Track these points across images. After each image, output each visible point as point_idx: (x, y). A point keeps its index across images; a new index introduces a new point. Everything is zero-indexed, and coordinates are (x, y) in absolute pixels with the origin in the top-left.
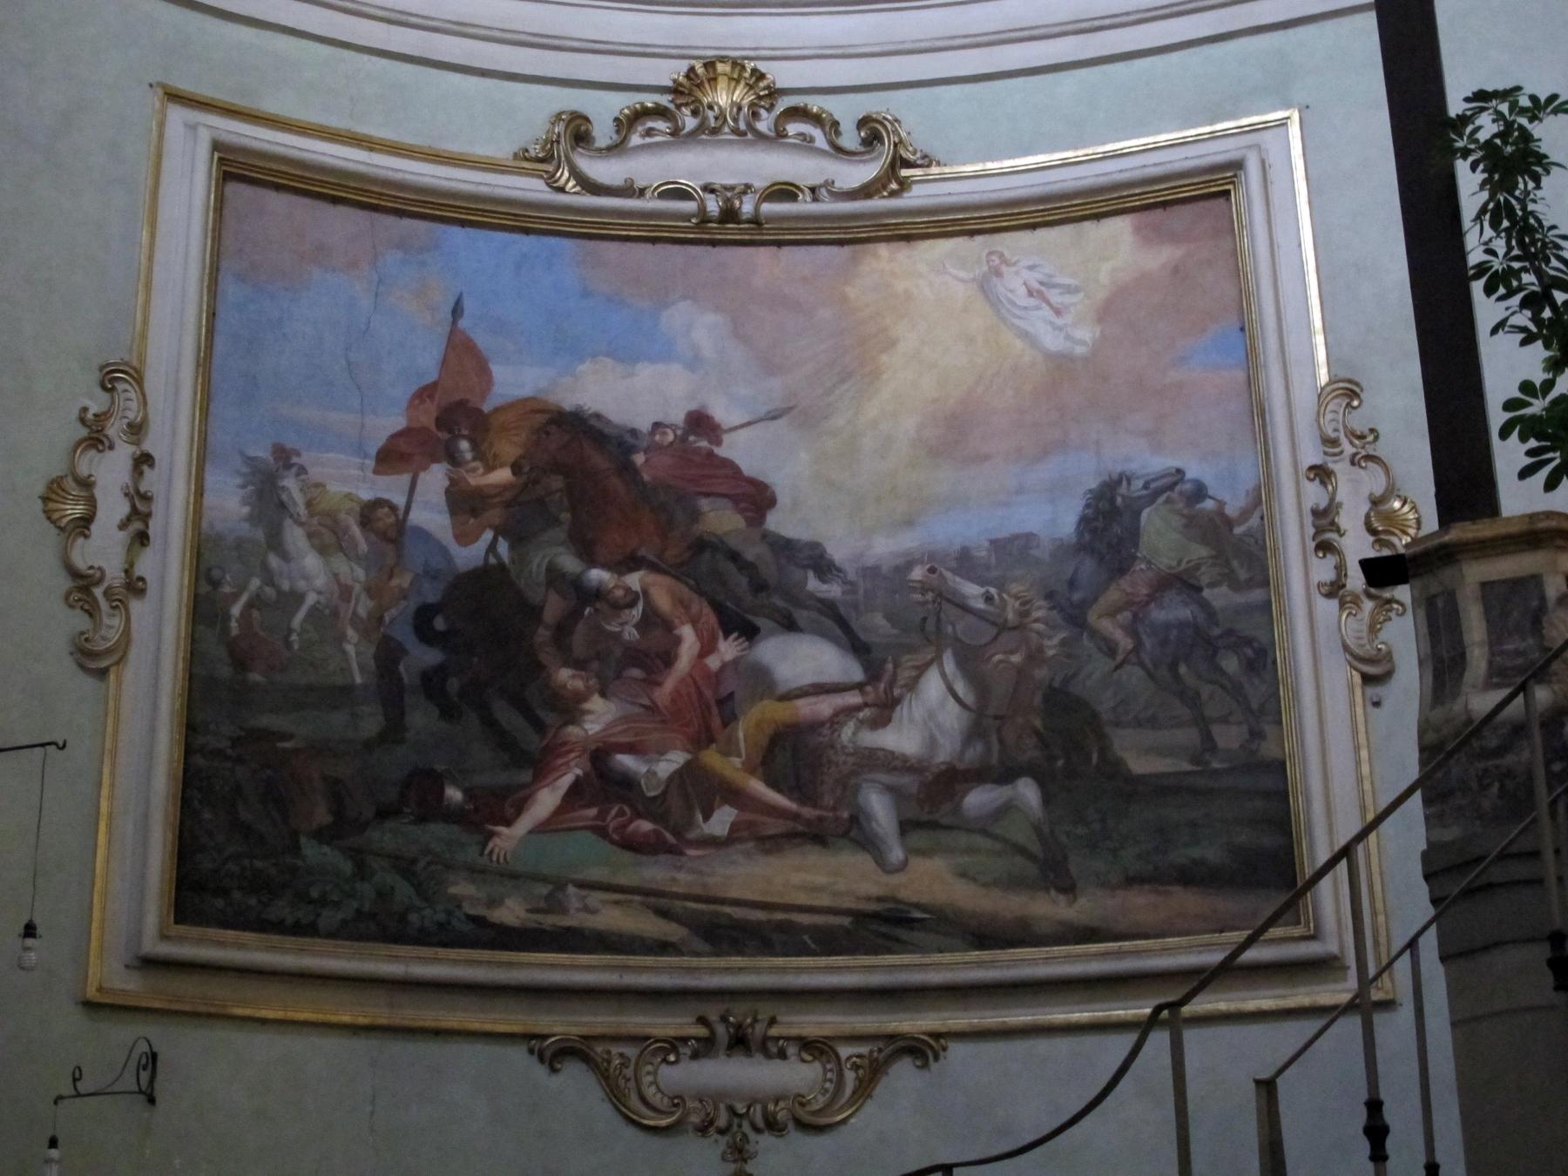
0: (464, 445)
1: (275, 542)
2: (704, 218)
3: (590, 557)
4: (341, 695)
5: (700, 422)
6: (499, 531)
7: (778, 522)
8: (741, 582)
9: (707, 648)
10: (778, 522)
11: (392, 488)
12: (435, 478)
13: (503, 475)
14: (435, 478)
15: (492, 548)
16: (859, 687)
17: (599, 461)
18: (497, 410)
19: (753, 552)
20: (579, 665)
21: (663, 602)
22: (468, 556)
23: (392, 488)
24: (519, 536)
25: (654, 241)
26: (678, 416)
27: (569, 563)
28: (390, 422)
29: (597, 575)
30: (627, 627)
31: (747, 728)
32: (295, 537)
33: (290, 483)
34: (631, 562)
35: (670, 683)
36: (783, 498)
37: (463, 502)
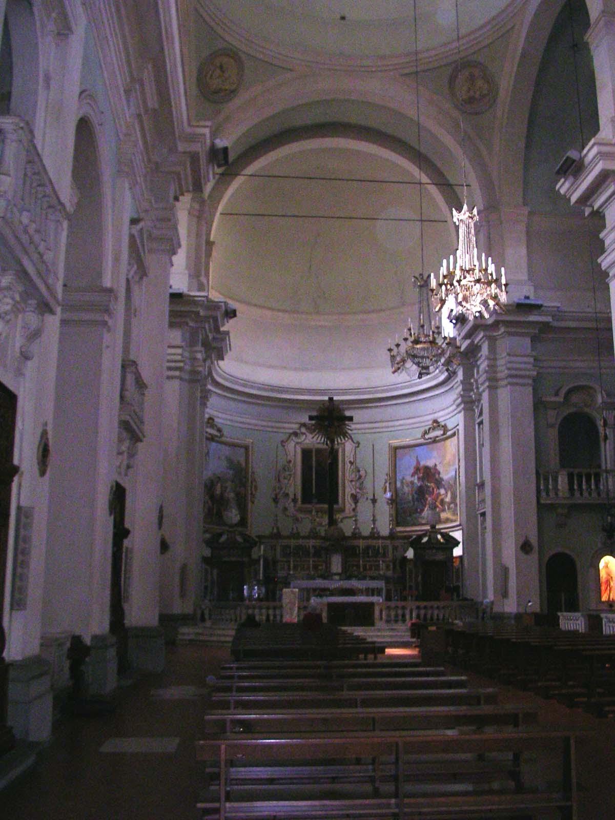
1: (403, 487)
4: (410, 502)
5: (436, 465)
11: (413, 479)
14: (416, 477)
19: (439, 480)
22: (419, 485)
23: (413, 479)
28: (412, 470)
30: (431, 489)
31: (439, 500)
32: (405, 487)
33: (404, 481)
37: (419, 478)
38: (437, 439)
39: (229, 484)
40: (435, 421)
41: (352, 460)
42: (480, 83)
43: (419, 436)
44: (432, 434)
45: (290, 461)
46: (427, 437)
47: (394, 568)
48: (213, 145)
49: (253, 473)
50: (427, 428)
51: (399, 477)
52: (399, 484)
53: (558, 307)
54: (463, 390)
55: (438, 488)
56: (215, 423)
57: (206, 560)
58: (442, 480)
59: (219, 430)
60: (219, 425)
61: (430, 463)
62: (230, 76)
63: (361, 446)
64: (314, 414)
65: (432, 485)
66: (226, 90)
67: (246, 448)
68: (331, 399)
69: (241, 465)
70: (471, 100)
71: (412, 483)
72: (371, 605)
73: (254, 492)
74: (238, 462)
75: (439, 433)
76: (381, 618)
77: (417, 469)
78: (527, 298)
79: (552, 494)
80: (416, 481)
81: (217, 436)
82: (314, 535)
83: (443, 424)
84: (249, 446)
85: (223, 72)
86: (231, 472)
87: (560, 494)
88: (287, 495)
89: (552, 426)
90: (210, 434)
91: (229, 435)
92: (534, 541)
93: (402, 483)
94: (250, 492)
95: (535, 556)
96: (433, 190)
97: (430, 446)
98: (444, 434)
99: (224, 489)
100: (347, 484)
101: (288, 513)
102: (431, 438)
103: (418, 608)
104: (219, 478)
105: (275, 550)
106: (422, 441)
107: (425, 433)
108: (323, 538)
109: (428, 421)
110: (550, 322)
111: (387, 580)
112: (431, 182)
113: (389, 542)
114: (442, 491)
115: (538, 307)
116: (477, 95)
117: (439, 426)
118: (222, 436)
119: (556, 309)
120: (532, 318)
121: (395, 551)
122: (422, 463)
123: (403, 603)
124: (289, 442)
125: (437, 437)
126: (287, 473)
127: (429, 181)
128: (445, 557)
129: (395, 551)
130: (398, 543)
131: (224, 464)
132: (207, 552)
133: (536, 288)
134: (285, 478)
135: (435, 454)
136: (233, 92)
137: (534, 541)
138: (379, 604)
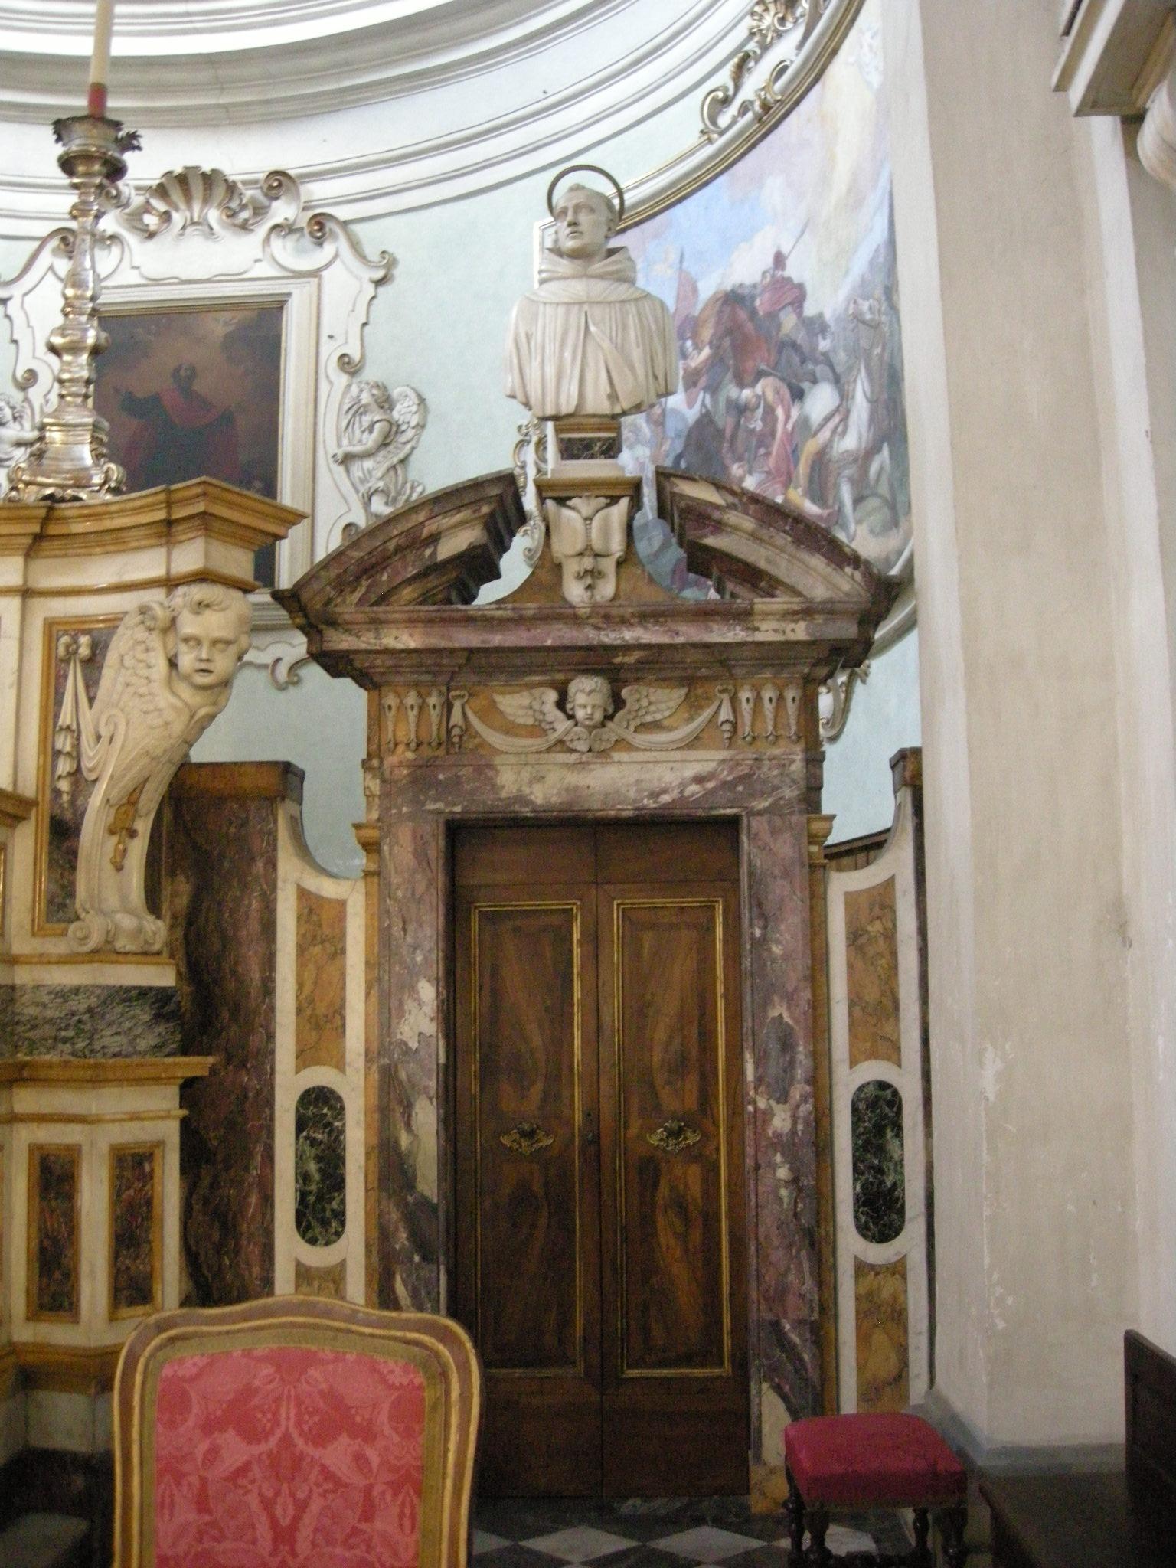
0: (689, 343)
2: (759, 119)
3: (742, 385)
5: (779, 260)
6: (705, 389)
7: (810, 309)
8: (796, 359)
9: (788, 417)
10: (810, 309)
13: (706, 352)
15: (703, 404)
16: (837, 410)
17: (742, 315)
18: (703, 310)
19: (801, 337)
20: (740, 459)
21: (770, 396)
22: (692, 415)
24: (713, 389)
25: (754, 146)
26: (769, 261)
27: (732, 391)
29: (747, 393)
34: (760, 375)
35: (775, 448)
36: (809, 289)
63: (397, 272)
65: (766, 387)
121: (74, 680)
128: (707, 760)
129: (74, 680)
135: (774, 192)
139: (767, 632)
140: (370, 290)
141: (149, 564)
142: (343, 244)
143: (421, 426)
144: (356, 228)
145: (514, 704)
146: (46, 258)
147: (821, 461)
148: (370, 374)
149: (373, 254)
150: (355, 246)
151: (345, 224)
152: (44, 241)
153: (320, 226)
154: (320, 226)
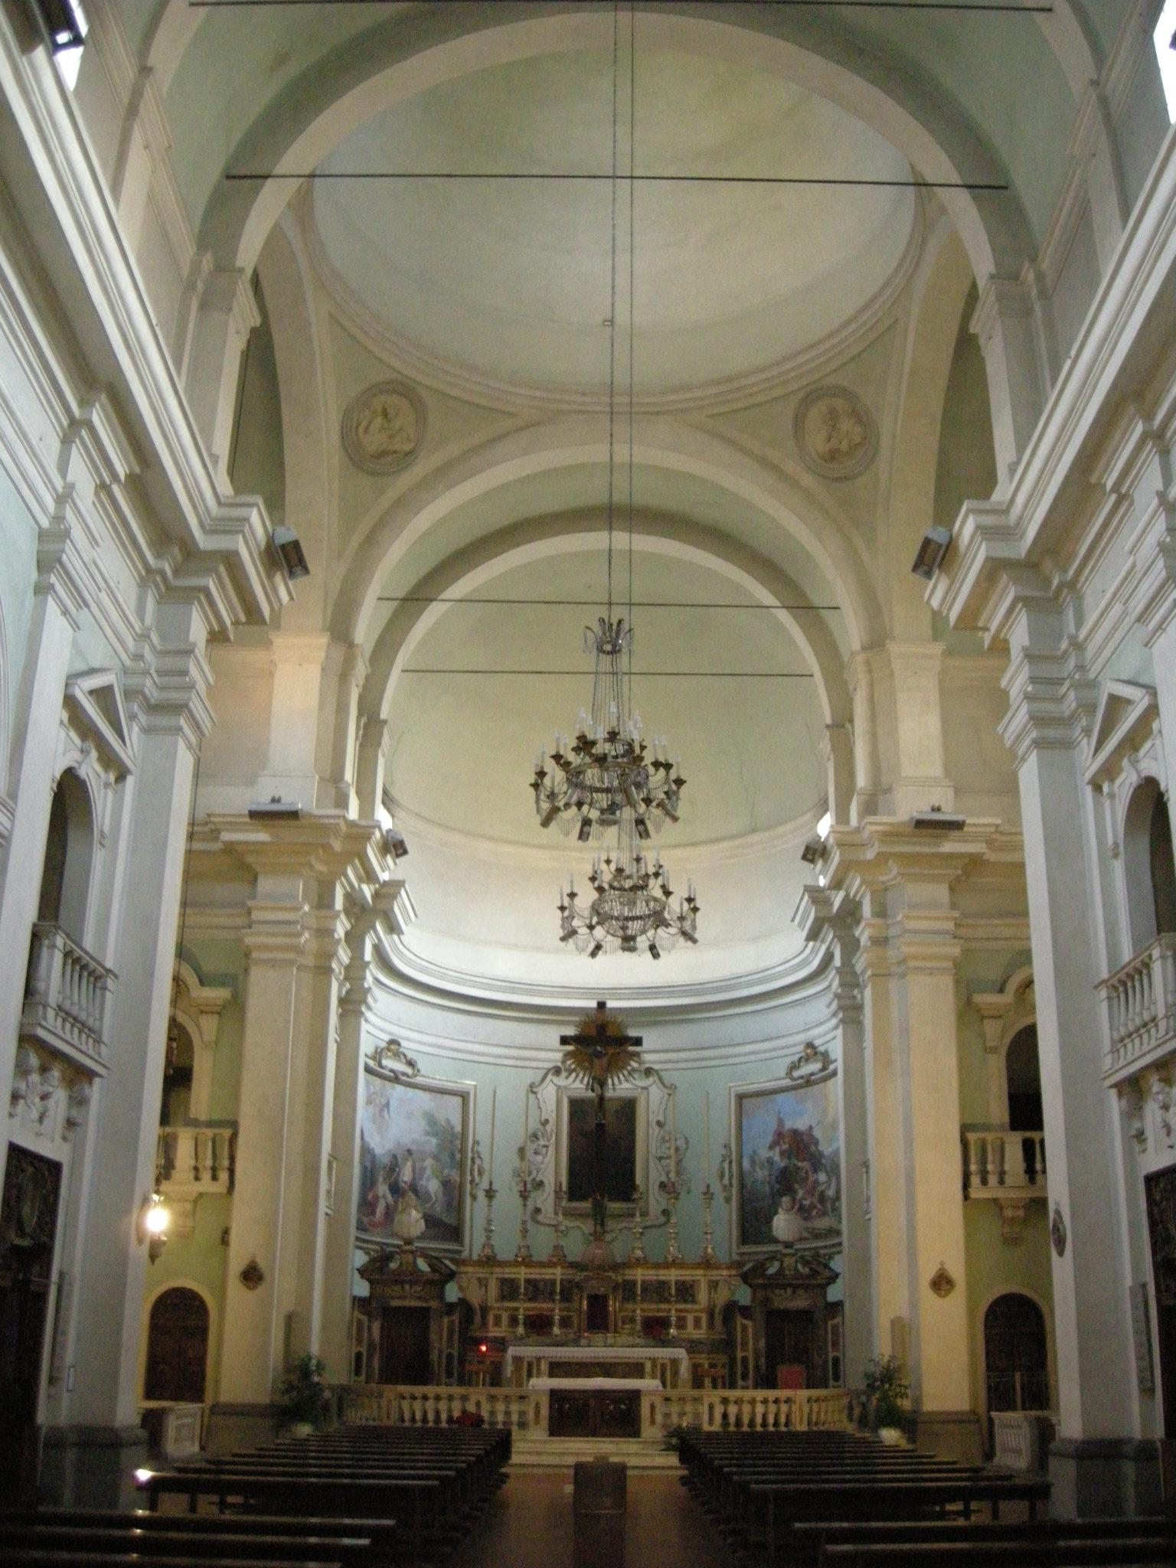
5: (811, 1128)
11: (770, 1154)
12: (777, 1150)
14: (777, 1150)
22: (782, 1165)
23: (770, 1154)
24: (789, 1158)
26: (807, 1127)
27: (796, 1162)
28: (770, 1139)
31: (817, 1194)
32: (758, 1169)
34: (804, 1160)
37: (782, 1153)
38: (813, 1078)
39: (429, 1162)
40: (810, 1045)
41: (661, 1118)
42: (846, 425)
43: (783, 1074)
44: (806, 1069)
45: (547, 1121)
46: (796, 1074)
47: (711, 1325)
48: (271, 540)
49: (476, 1143)
50: (796, 1058)
51: (747, 1150)
52: (746, 1164)
53: (997, 826)
54: (842, 985)
55: (815, 1171)
56: (401, 1050)
57: (360, 1303)
58: (821, 1154)
59: (411, 1063)
60: (410, 1055)
61: (801, 1125)
62: (401, 429)
64: (571, 1031)
66: (395, 452)
67: (464, 1096)
68: (602, 1005)
69: (453, 1128)
70: (833, 456)
71: (770, 1161)
72: (635, 1396)
73: (477, 1179)
74: (448, 1121)
75: (815, 1067)
76: (653, 1421)
77: (779, 1135)
78: (937, 809)
79: (993, 1180)
80: (777, 1158)
81: (404, 1074)
82: (559, 1257)
83: (822, 1049)
84: (468, 1093)
85: (389, 421)
86: (434, 1141)
87: (1008, 1180)
88: (541, 1184)
89: (994, 1050)
90: (392, 1071)
91: (433, 1072)
92: (957, 1271)
93: (753, 1162)
94: (469, 1178)
95: (958, 1298)
96: (784, 616)
97: (802, 1091)
98: (824, 1068)
99: (417, 1173)
100: (652, 1165)
101: (540, 1218)
102: (802, 1077)
103: (725, 1401)
104: (409, 1152)
105: (486, 1286)
106: (787, 1082)
107: (794, 1067)
108: (573, 1265)
109: (795, 1045)
110: (984, 854)
111: (693, 1347)
112: (779, 604)
113: (701, 1272)
114: (822, 1177)
115: (957, 826)
116: (844, 446)
117: (816, 1053)
118: (417, 1072)
119: (992, 829)
120: (947, 847)
122: (789, 1124)
123: (695, 1393)
124: (544, 1085)
125: (812, 1074)
126: (542, 1142)
127: (779, 604)
130: (715, 1275)
131: (422, 1124)
132: (362, 1289)
133: (958, 792)
134: (536, 1153)
136: (409, 457)
137: (957, 1271)
138: (650, 1393)
139: (819, 1282)
140: (666, 1097)
141: (725, 1272)
142: (656, 1078)
143: (687, 1149)
144: (662, 1073)
145: (777, 1292)
146: (550, 1077)
147: (822, 1195)
148: (667, 1128)
149: (666, 1082)
150: (660, 1079)
151: (657, 1071)
152: (550, 1070)
153: (648, 1072)
154: (648, 1072)
